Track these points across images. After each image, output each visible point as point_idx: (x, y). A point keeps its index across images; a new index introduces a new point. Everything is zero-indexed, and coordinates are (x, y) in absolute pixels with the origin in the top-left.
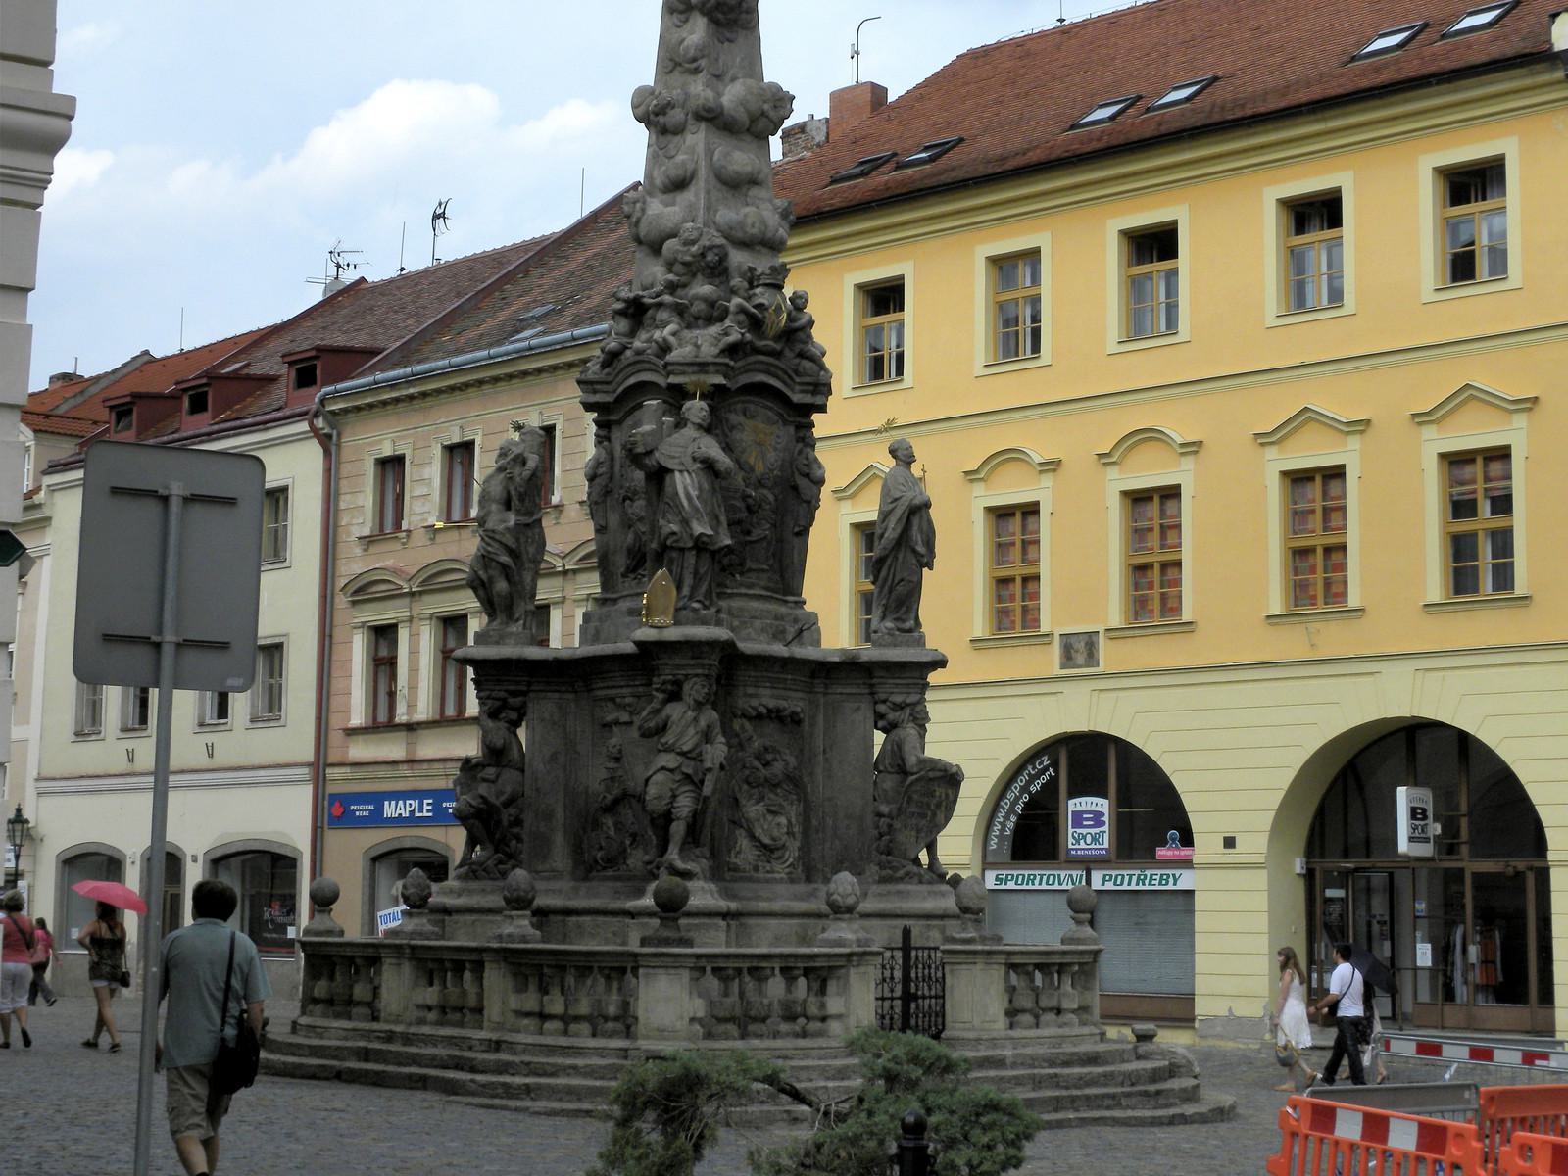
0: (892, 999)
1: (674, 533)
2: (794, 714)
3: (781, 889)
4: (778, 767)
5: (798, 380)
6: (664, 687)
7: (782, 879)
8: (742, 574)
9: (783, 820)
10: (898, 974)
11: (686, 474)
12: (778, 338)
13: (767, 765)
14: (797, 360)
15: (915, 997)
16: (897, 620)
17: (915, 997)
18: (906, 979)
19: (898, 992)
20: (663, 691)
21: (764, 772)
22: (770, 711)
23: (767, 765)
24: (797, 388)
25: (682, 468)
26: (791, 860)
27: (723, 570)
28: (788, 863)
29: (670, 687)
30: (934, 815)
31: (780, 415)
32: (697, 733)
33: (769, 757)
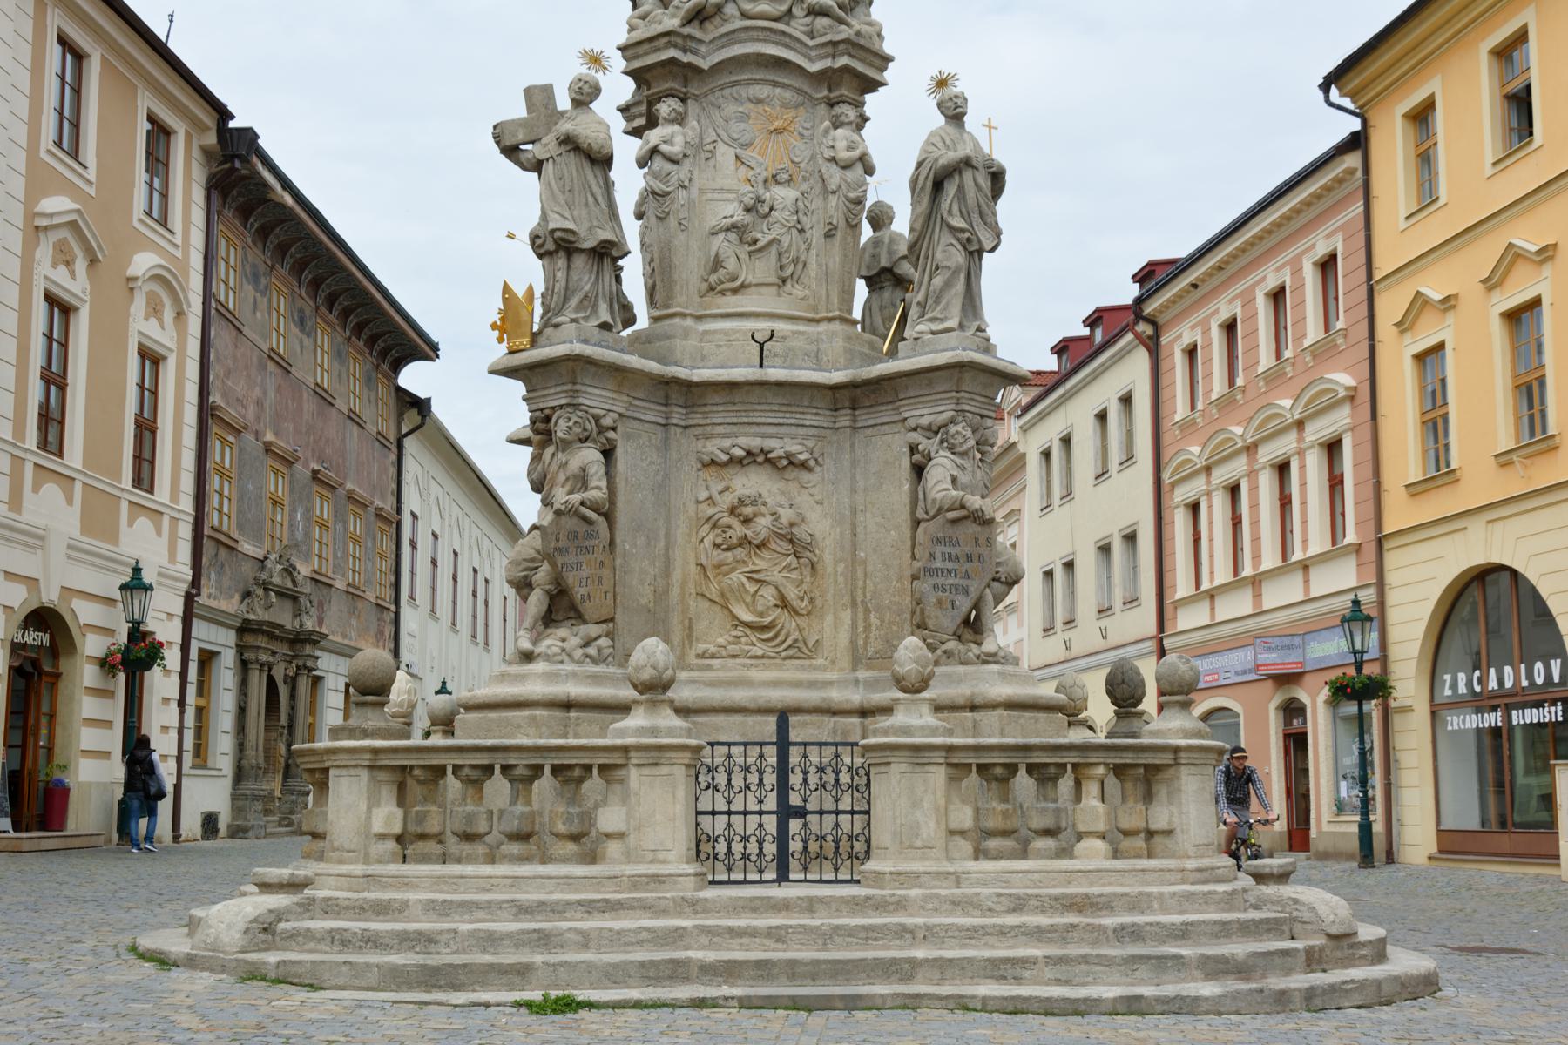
0: (837, 813)
4: (763, 524)
5: (811, 43)
10: (770, 779)
13: (746, 521)
15: (801, 813)
17: (801, 813)
18: (783, 787)
19: (771, 803)
21: (739, 530)
22: (749, 453)
23: (746, 521)
24: (813, 53)
26: (789, 642)
27: (712, 289)
31: (800, 91)
32: (567, 479)
33: (748, 511)
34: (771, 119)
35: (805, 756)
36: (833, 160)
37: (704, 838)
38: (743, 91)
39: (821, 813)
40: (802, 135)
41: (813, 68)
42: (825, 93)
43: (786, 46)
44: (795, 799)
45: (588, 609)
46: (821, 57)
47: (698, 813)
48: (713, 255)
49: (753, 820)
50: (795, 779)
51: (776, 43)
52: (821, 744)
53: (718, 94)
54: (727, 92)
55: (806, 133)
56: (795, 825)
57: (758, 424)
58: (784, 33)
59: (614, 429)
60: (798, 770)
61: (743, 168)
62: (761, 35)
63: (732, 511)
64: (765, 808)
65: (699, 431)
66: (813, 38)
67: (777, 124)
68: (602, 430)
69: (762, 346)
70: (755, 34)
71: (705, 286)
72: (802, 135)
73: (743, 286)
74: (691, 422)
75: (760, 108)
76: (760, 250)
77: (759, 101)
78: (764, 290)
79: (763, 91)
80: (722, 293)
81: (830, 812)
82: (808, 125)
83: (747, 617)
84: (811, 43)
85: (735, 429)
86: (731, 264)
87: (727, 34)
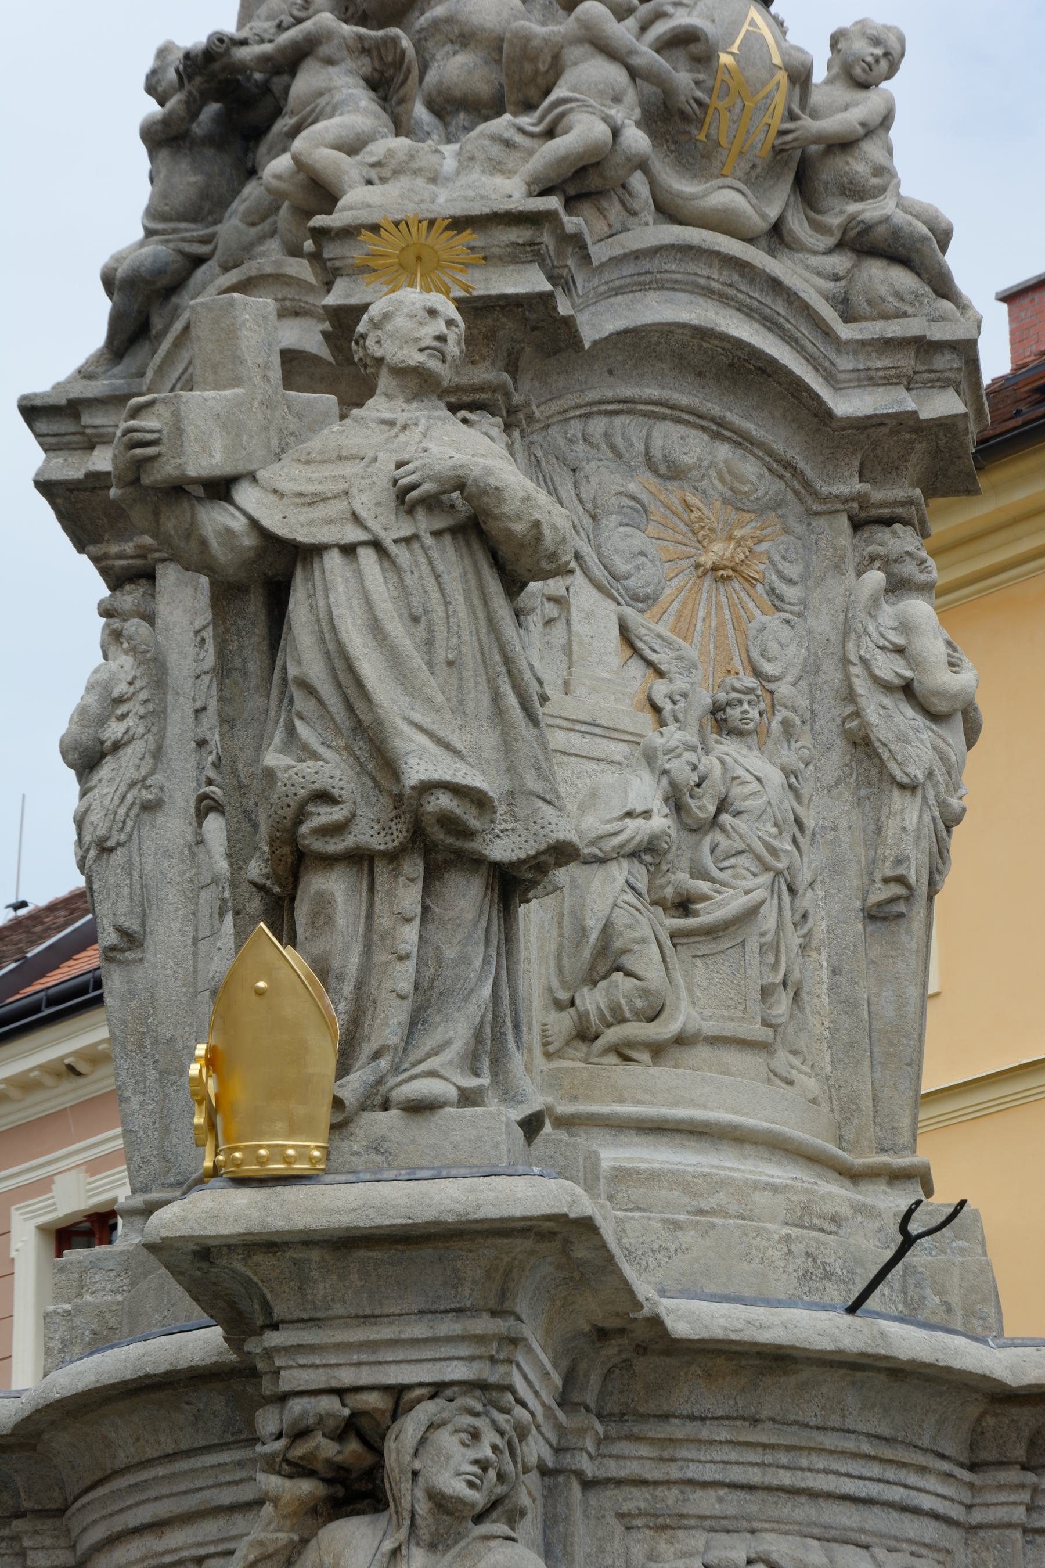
1: (325, 797)
5: (845, 332)
6: (300, 1450)
11: (367, 557)
12: (756, 180)
14: (840, 262)
20: (300, 1469)
24: (845, 363)
25: (352, 534)
27: (584, 1035)
29: (328, 1449)
31: (783, 467)
34: (700, 533)
36: (907, 690)
38: (630, 430)
40: (777, 599)
41: (849, 404)
42: (855, 486)
43: (771, 324)
46: (870, 380)
48: (594, 926)
51: (747, 311)
53: (575, 428)
54: (598, 426)
55: (791, 593)
57: (813, 1494)
58: (775, 285)
61: (636, 668)
62: (717, 277)
65: (637, 1500)
66: (848, 318)
67: (718, 551)
70: (701, 270)
71: (562, 1023)
72: (777, 599)
73: (681, 1041)
74: (613, 1469)
75: (674, 494)
76: (711, 932)
77: (673, 472)
78: (733, 1058)
79: (690, 446)
80: (623, 1052)
82: (793, 571)
84: (845, 332)
85: (752, 1504)
86: (648, 962)
87: (637, 255)
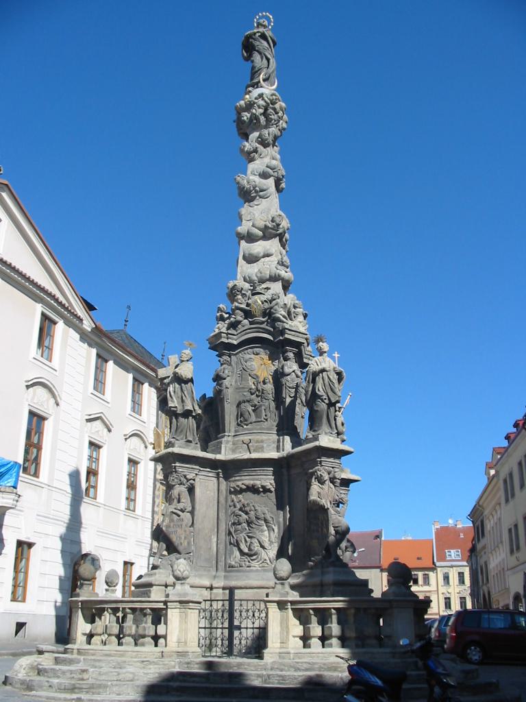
2: (263, 487)
3: (252, 575)
7: (257, 571)
8: (247, 425)
9: (255, 541)
10: (226, 615)
13: (247, 513)
15: (239, 628)
16: (314, 431)
17: (239, 628)
19: (226, 625)
22: (247, 486)
28: (261, 562)
30: (322, 530)
35: (211, 606)
37: (201, 638)
39: (247, 628)
44: (236, 623)
45: (180, 548)
47: (200, 628)
49: (219, 631)
50: (237, 614)
52: (247, 600)
56: (236, 633)
59: (194, 480)
60: (238, 611)
63: (240, 509)
64: (224, 626)
68: (188, 480)
69: (248, 445)
81: (250, 628)
83: (246, 550)
